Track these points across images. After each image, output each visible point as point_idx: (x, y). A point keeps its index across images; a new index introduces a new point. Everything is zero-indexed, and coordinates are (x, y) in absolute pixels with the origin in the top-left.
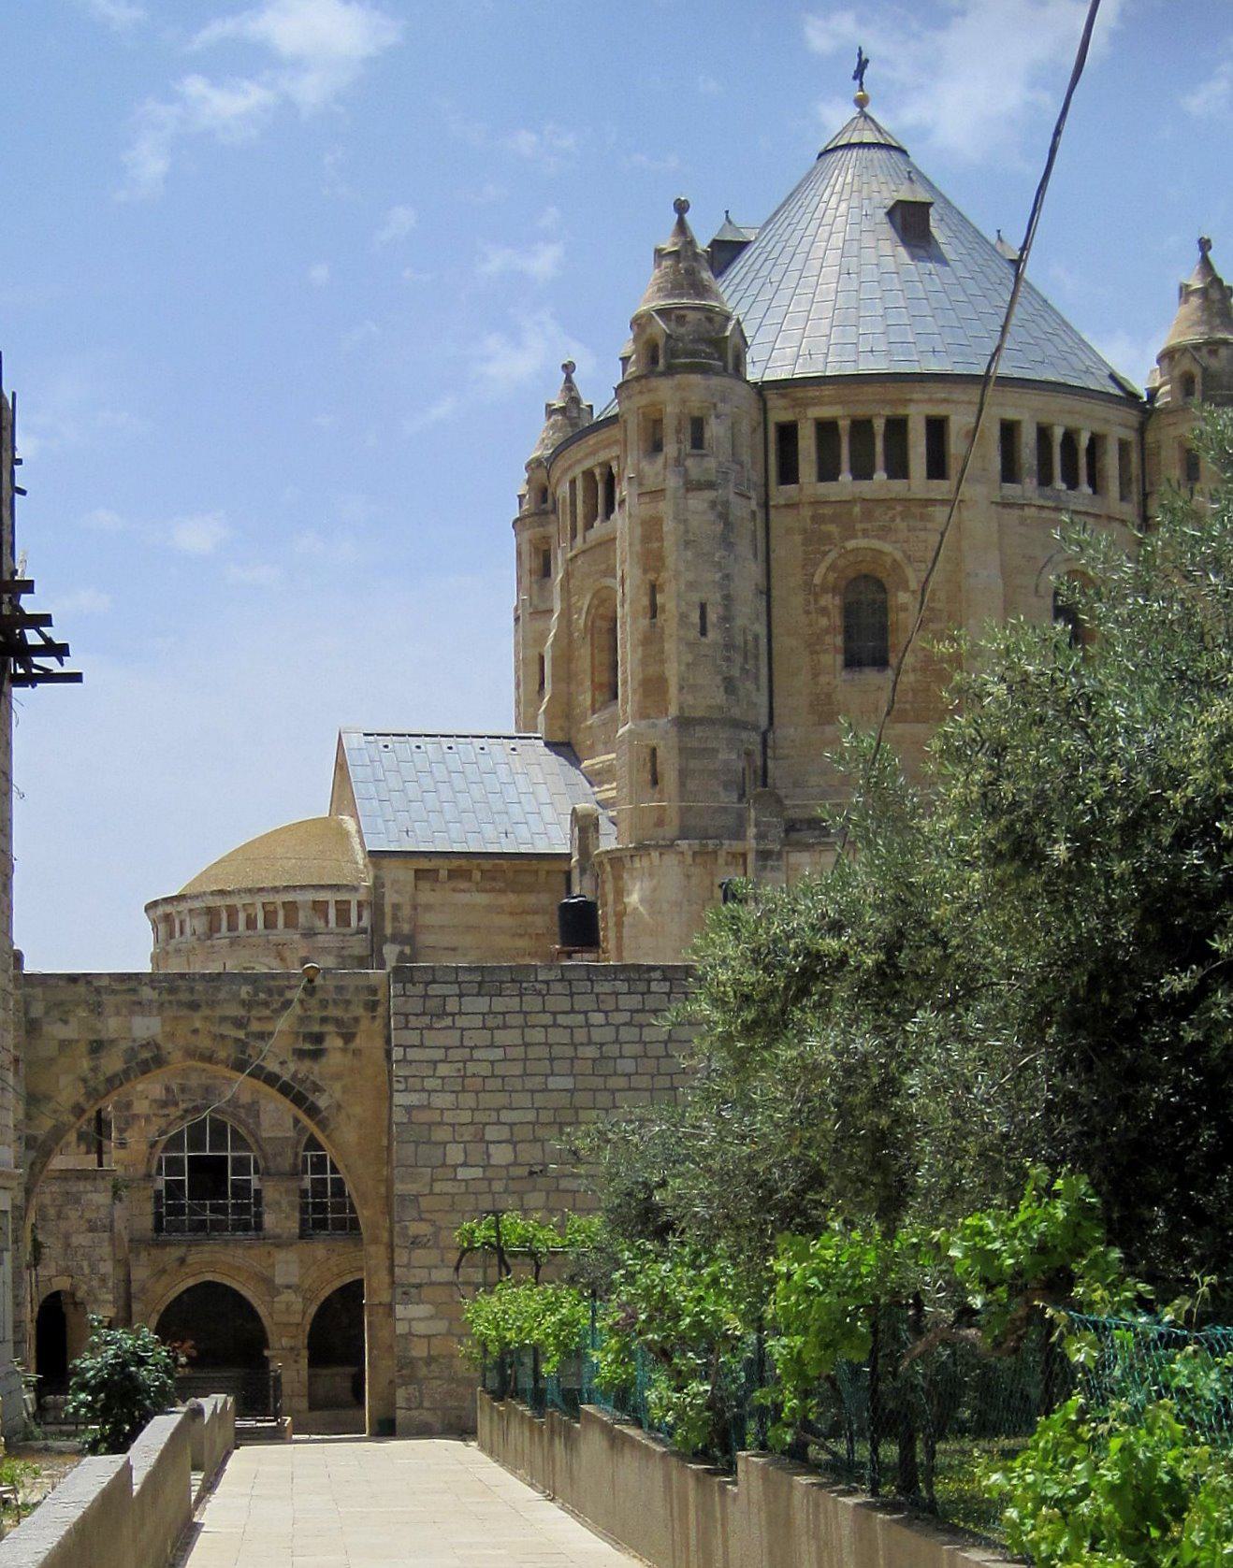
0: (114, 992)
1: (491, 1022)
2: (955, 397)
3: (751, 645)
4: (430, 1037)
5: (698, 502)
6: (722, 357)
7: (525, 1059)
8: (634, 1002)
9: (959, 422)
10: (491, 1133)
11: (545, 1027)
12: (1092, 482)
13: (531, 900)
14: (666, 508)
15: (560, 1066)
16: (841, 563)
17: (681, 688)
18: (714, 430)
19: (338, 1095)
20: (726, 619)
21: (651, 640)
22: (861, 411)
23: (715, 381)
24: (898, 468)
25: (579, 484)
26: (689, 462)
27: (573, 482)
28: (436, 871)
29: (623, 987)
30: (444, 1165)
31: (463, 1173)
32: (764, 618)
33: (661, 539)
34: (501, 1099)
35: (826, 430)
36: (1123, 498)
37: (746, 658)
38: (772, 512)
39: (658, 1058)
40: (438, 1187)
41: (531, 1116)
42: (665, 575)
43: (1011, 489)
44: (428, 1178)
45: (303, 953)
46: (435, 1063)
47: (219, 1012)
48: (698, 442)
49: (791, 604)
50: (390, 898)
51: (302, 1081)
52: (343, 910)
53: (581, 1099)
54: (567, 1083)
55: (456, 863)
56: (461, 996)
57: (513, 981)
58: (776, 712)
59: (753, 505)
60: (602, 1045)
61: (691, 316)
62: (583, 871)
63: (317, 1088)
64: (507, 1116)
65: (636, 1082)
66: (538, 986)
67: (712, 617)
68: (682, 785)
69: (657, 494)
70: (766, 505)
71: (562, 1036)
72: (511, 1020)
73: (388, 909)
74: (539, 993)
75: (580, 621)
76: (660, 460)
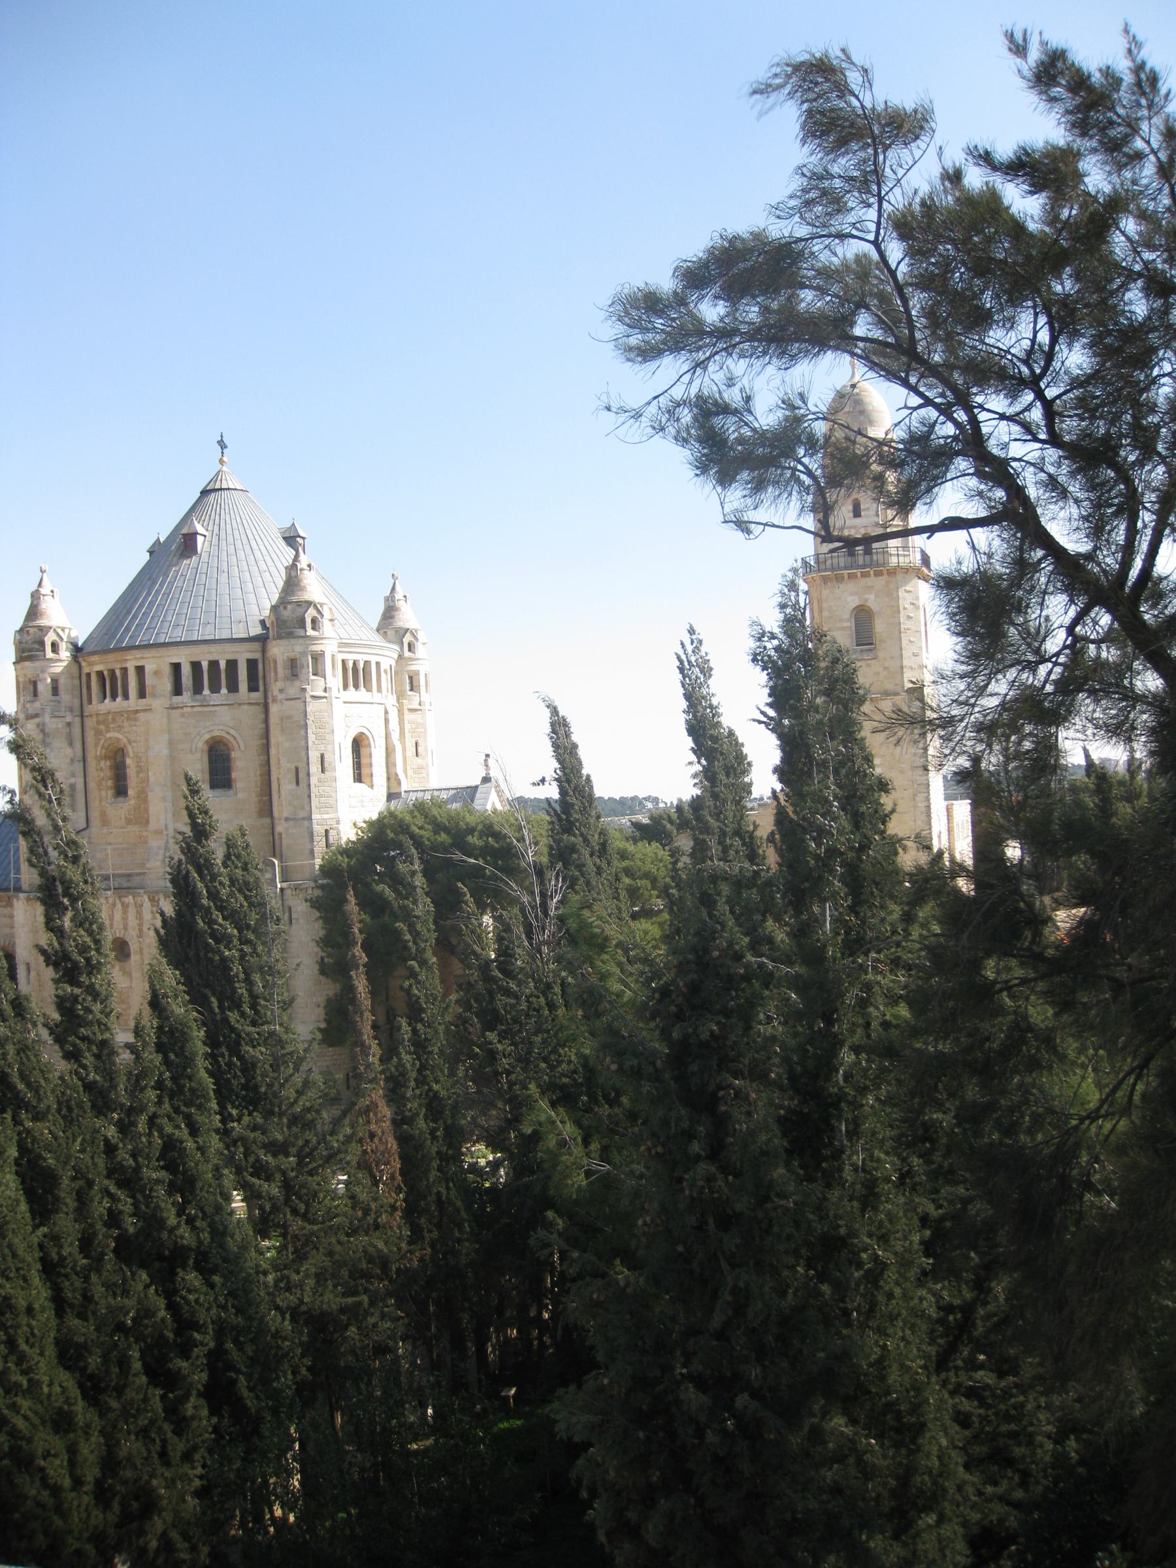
9: (149, 668)
22: (110, 667)
23: (37, 664)
24: (126, 696)
26: (28, 705)
38: (86, 720)
43: (177, 699)
70: (82, 716)
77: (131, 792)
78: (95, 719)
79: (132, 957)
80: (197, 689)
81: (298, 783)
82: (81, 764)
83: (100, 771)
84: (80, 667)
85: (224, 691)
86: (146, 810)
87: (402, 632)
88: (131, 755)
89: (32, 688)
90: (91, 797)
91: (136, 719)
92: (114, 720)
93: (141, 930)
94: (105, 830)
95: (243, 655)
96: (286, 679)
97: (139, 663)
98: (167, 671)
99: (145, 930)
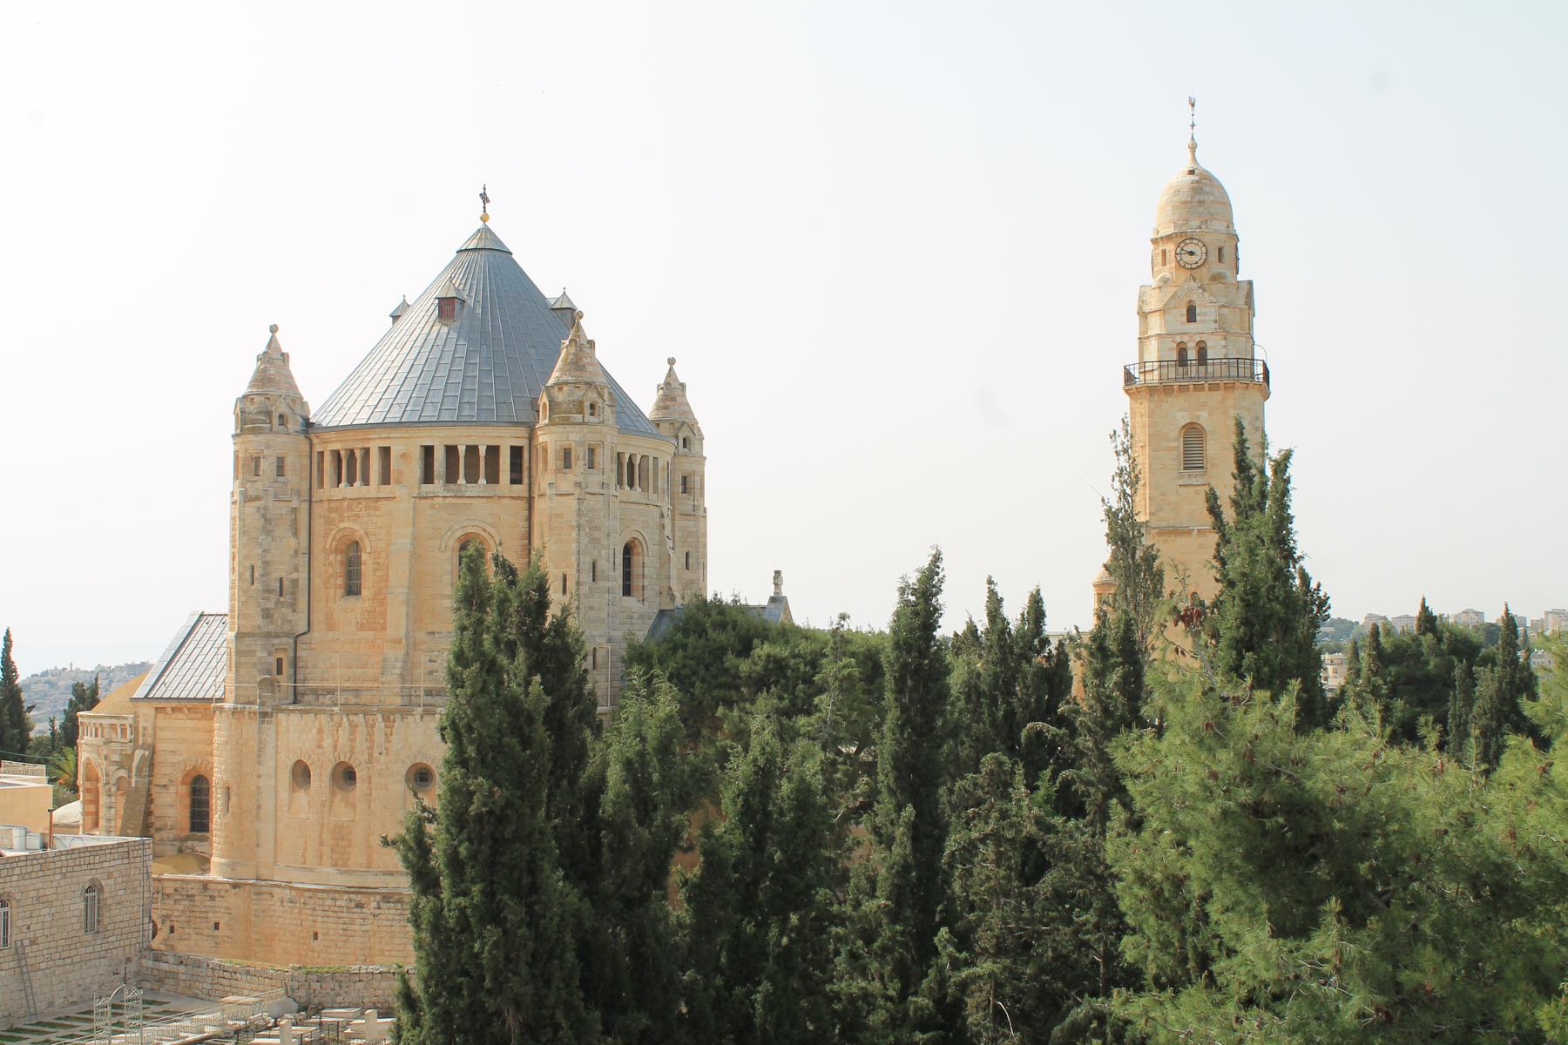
2: (392, 435)
5: (251, 508)
6: (270, 422)
16: (338, 536)
17: (239, 616)
22: (350, 446)
23: (261, 438)
24: (366, 481)
26: (248, 485)
35: (337, 454)
38: (314, 506)
43: (427, 488)
45: (105, 753)
50: (142, 724)
52: (123, 731)
55: (174, 704)
61: (257, 399)
67: (257, 574)
68: (237, 672)
73: (141, 730)
78: (326, 505)
79: (358, 785)
80: (451, 477)
81: (564, 592)
82: (307, 556)
83: (329, 568)
84: (311, 445)
85: (482, 481)
86: (383, 614)
87: (677, 425)
88: (369, 550)
89: (253, 465)
90: (315, 596)
91: (376, 509)
92: (350, 508)
93: (370, 755)
94: (331, 634)
95: (507, 439)
96: (558, 471)
98: (417, 454)
99: (376, 755)
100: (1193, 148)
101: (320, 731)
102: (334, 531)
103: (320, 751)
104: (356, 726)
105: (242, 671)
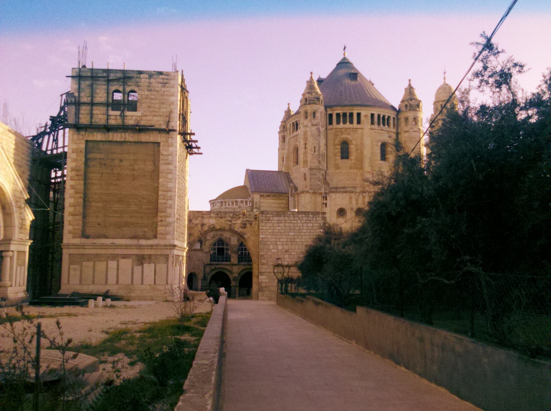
0: (206, 215)
1: (279, 222)
3: (323, 154)
4: (267, 225)
5: (314, 128)
7: (285, 229)
8: (306, 218)
9: (363, 113)
10: (278, 243)
11: (289, 223)
12: (388, 125)
13: (282, 201)
14: (308, 129)
15: (292, 231)
17: (310, 162)
18: (318, 115)
19: (249, 235)
20: (319, 150)
21: (305, 153)
22: (344, 111)
23: (318, 106)
24: (351, 122)
25: (291, 125)
26: (313, 121)
27: (290, 125)
28: (264, 196)
29: (304, 216)
30: (269, 249)
31: (273, 251)
32: (326, 150)
33: (307, 135)
34: (280, 237)
35: (338, 115)
36: (394, 128)
37: (322, 157)
38: (328, 131)
39: (310, 229)
40: (268, 253)
41: (286, 240)
42: (308, 142)
43: (373, 126)
44: (266, 252)
46: (268, 229)
47: (226, 219)
48: (314, 117)
49: (331, 147)
50: (255, 200)
51: (242, 232)
52: (246, 202)
53: (296, 237)
54: (293, 234)
56: (273, 217)
57: (283, 214)
58: (328, 167)
59: (324, 129)
60: (300, 227)
62: (291, 196)
63: (245, 234)
64: (281, 240)
65: (307, 234)
66: (288, 215)
67: (316, 149)
68: (310, 180)
69: (307, 126)
70: (326, 129)
71: (292, 225)
72: (283, 221)
73: (255, 203)
74: (288, 217)
75: (291, 150)
76: (307, 120)
77: (353, 157)
78: (334, 130)
84: (326, 111)
88: (354, 144)
92: (345, 131)
94: (338, 171)
97: (359, 111)
98: (370, 116)
100: (445, 78)
101: (351, 198)
102: (339, 138)
103: (351, 204)
104: (365, 197)
105: (312, 180)
